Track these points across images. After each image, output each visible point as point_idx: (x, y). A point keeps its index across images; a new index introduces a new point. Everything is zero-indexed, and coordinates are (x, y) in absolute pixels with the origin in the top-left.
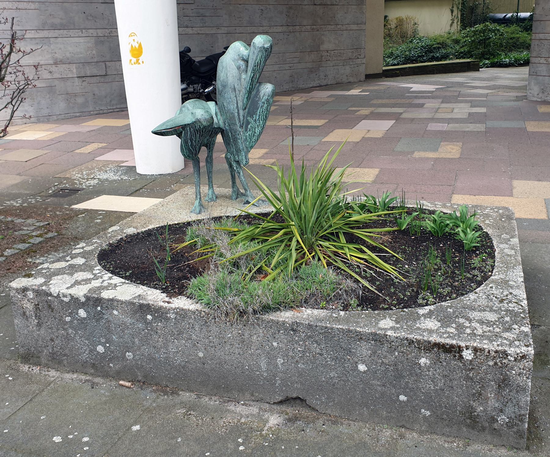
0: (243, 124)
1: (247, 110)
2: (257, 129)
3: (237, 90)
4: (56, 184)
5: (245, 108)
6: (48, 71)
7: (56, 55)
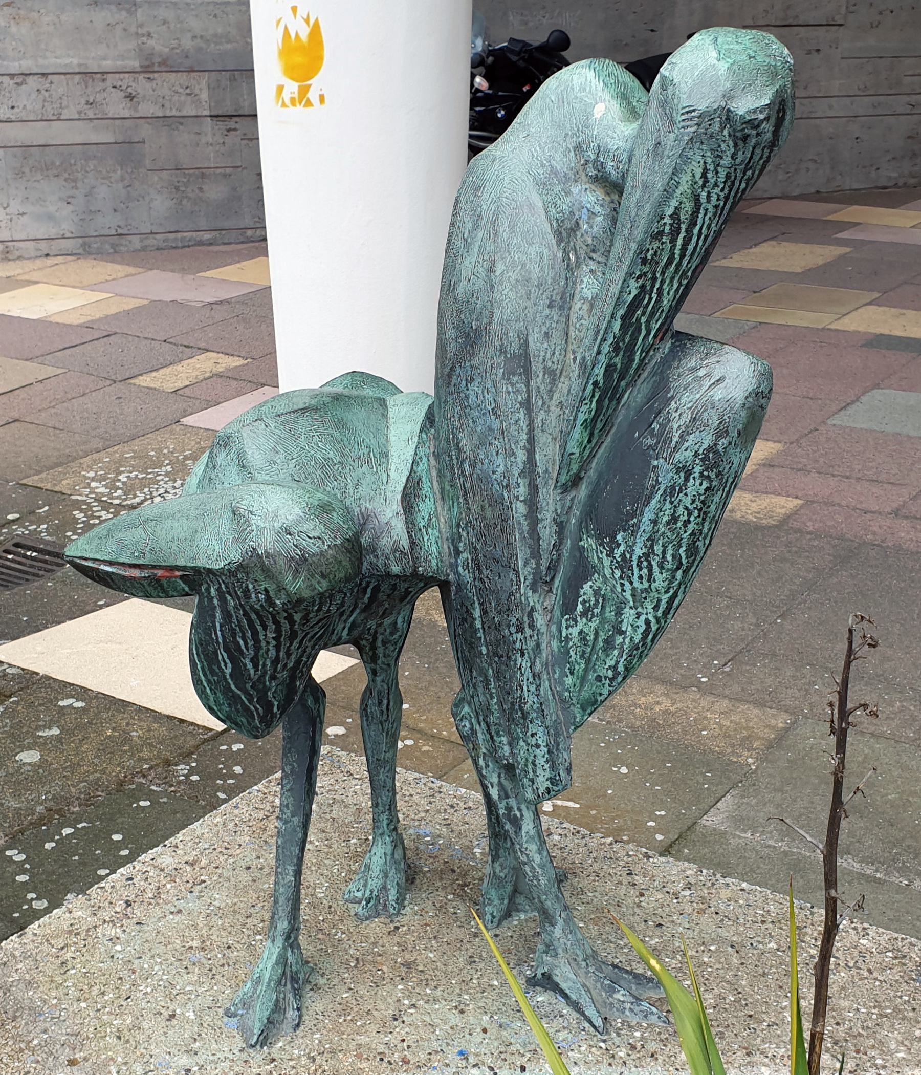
0: (553, 568)
1: (583, 491)
2: (629, 614)
3: (537, 367)
4: (10, 517)
5: (576, 481)
6: (122, 94)
7: (151, 42)
